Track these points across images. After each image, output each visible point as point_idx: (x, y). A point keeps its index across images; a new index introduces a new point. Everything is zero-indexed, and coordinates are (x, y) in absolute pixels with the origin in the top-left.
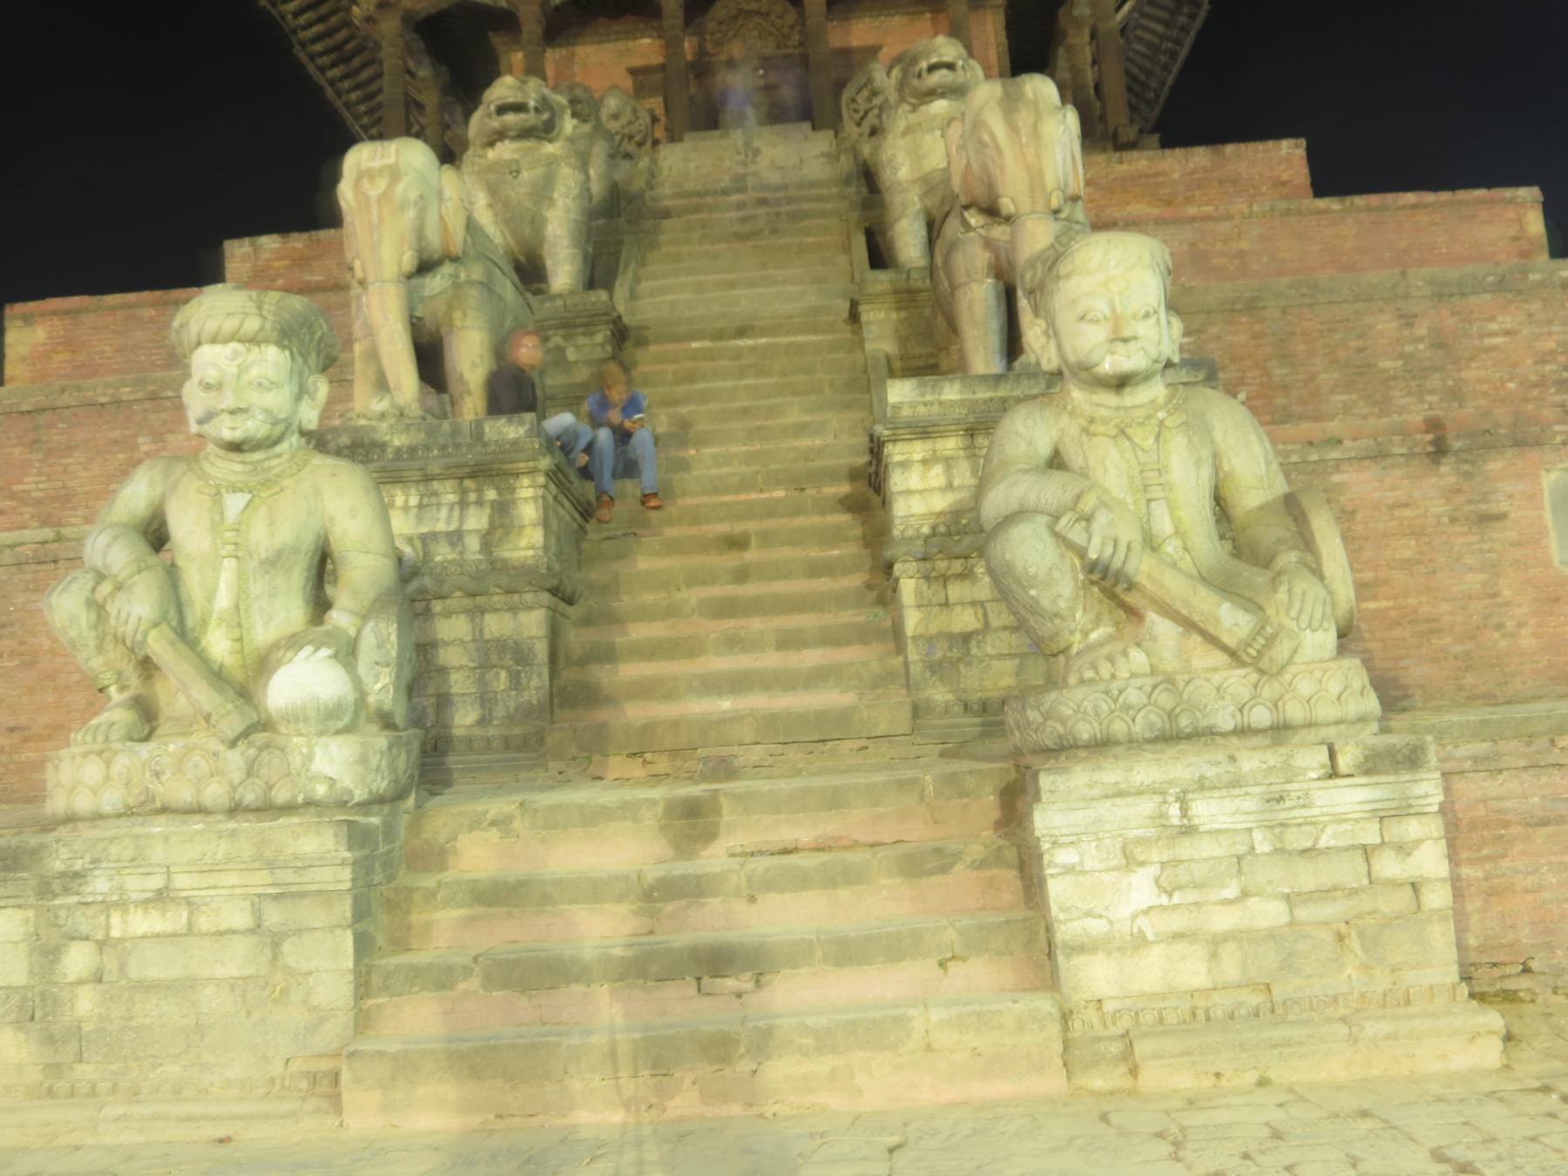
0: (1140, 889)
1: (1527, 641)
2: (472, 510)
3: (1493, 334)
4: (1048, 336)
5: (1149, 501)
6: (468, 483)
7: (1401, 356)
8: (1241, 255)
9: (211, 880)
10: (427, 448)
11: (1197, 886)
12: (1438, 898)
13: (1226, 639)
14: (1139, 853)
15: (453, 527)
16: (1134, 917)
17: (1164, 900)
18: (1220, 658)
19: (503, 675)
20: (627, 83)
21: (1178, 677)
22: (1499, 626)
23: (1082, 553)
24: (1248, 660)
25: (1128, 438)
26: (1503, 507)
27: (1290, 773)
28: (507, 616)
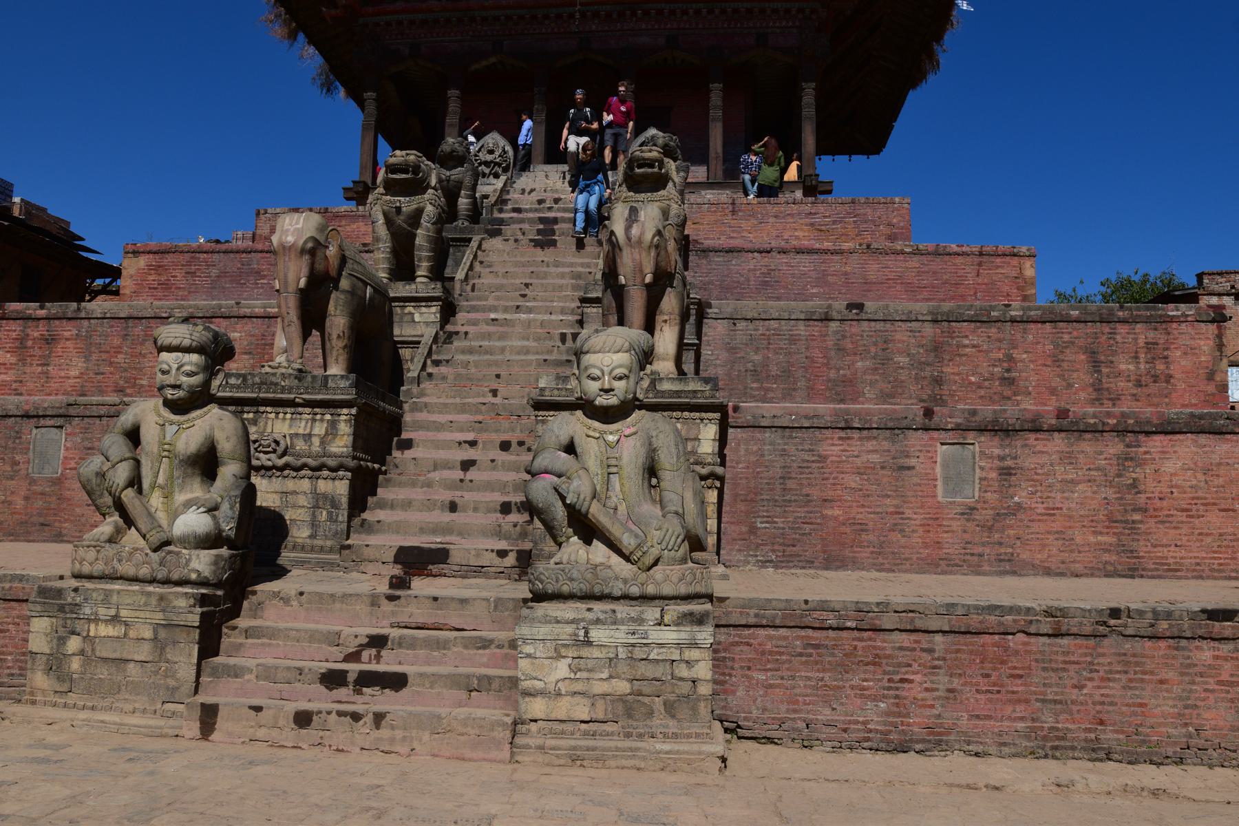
0: (562, 669)
1: (916, 539)
2: (317, 423)
6: (317, 410)
8: (846, 274)
9: (138, 614)
10: (298, 388)
11: (589, 671)
12: (705, 690)
14: (563, 652)
15: (307, 431)
16: (557, 682)
17: (572, 676)
19: (324, 513)
22: (902, 531)
23: (563, 498)
26: (913, 462)
27: (640, 621)
28: (330, 482)
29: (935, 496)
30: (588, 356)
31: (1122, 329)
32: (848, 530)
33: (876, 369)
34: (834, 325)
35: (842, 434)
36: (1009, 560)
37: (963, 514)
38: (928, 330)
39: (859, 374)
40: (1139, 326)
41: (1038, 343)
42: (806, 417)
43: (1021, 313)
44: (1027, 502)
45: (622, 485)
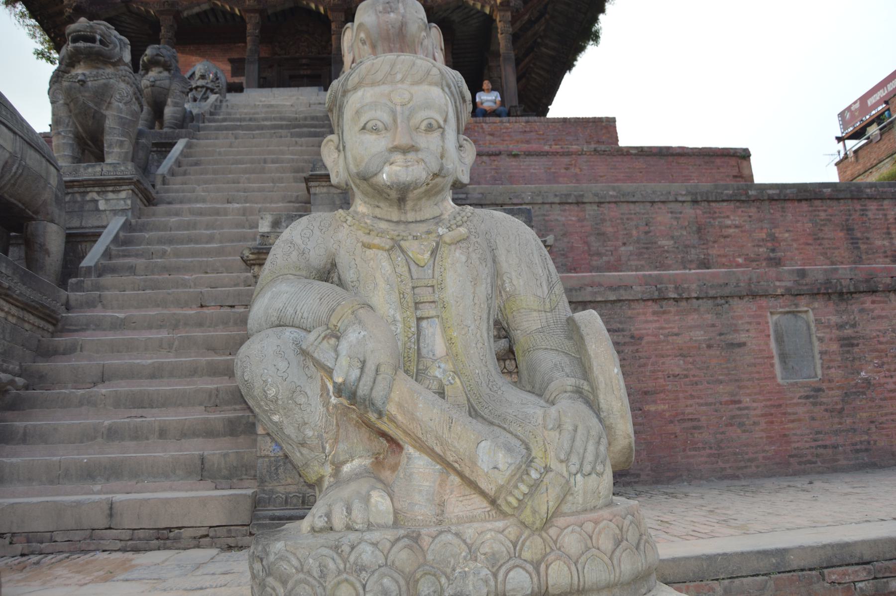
3: (729, 227)
4: (339, 151)
5: (419, 319)
7: (672, 238)
8: (576, 174)
13: (483, 485)
18: (479, 505)
20: (228, 67)
21: (424, 531)
22: (741, 425)
24: (505, 508)
25: (403, 251)
26: (742, 337)
29: (774, 378)
30: (360, 93)
31: (872, 206)
32: (677, 428)
33: (641, 254)
34: (591, 210)
35: (656, 307)
36: (867, 450)
37: (807, 397)
38: (689, 211)
39: (624, 259)
40: (886, 202)
41: (797, 221)
42: (611, 288)
43: (777, 191)
44: (877, 378)
45: (450, 342)
